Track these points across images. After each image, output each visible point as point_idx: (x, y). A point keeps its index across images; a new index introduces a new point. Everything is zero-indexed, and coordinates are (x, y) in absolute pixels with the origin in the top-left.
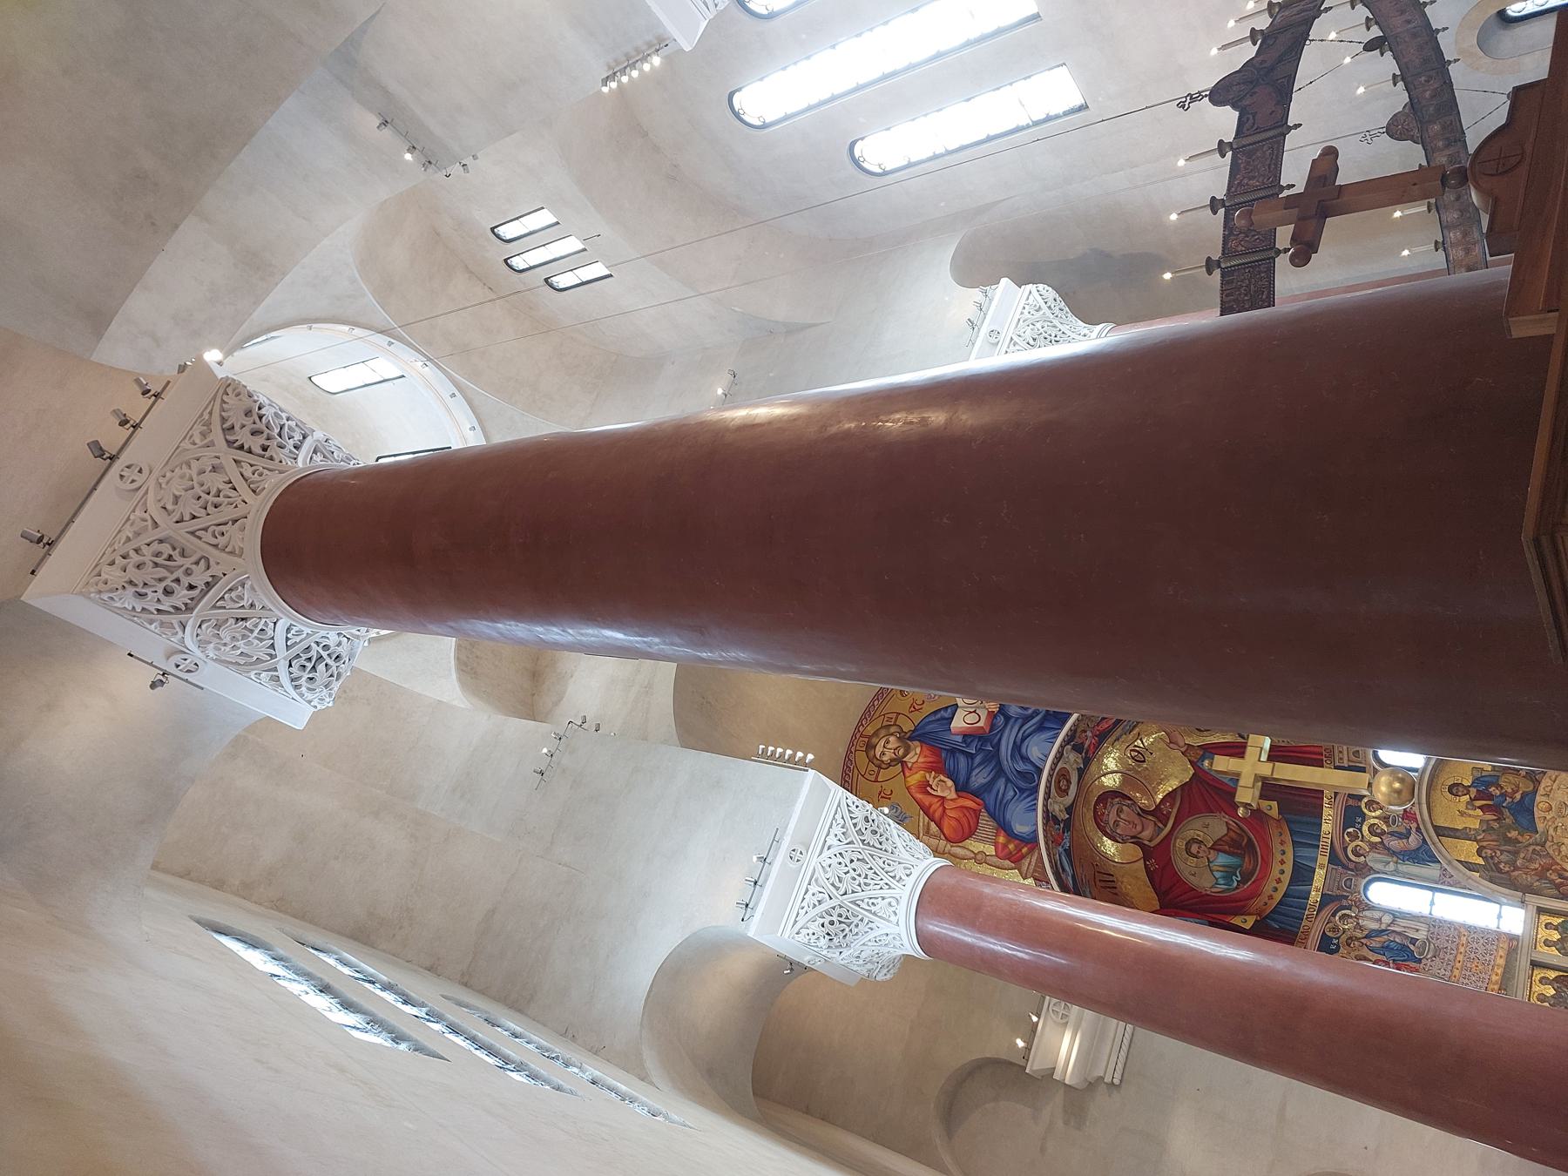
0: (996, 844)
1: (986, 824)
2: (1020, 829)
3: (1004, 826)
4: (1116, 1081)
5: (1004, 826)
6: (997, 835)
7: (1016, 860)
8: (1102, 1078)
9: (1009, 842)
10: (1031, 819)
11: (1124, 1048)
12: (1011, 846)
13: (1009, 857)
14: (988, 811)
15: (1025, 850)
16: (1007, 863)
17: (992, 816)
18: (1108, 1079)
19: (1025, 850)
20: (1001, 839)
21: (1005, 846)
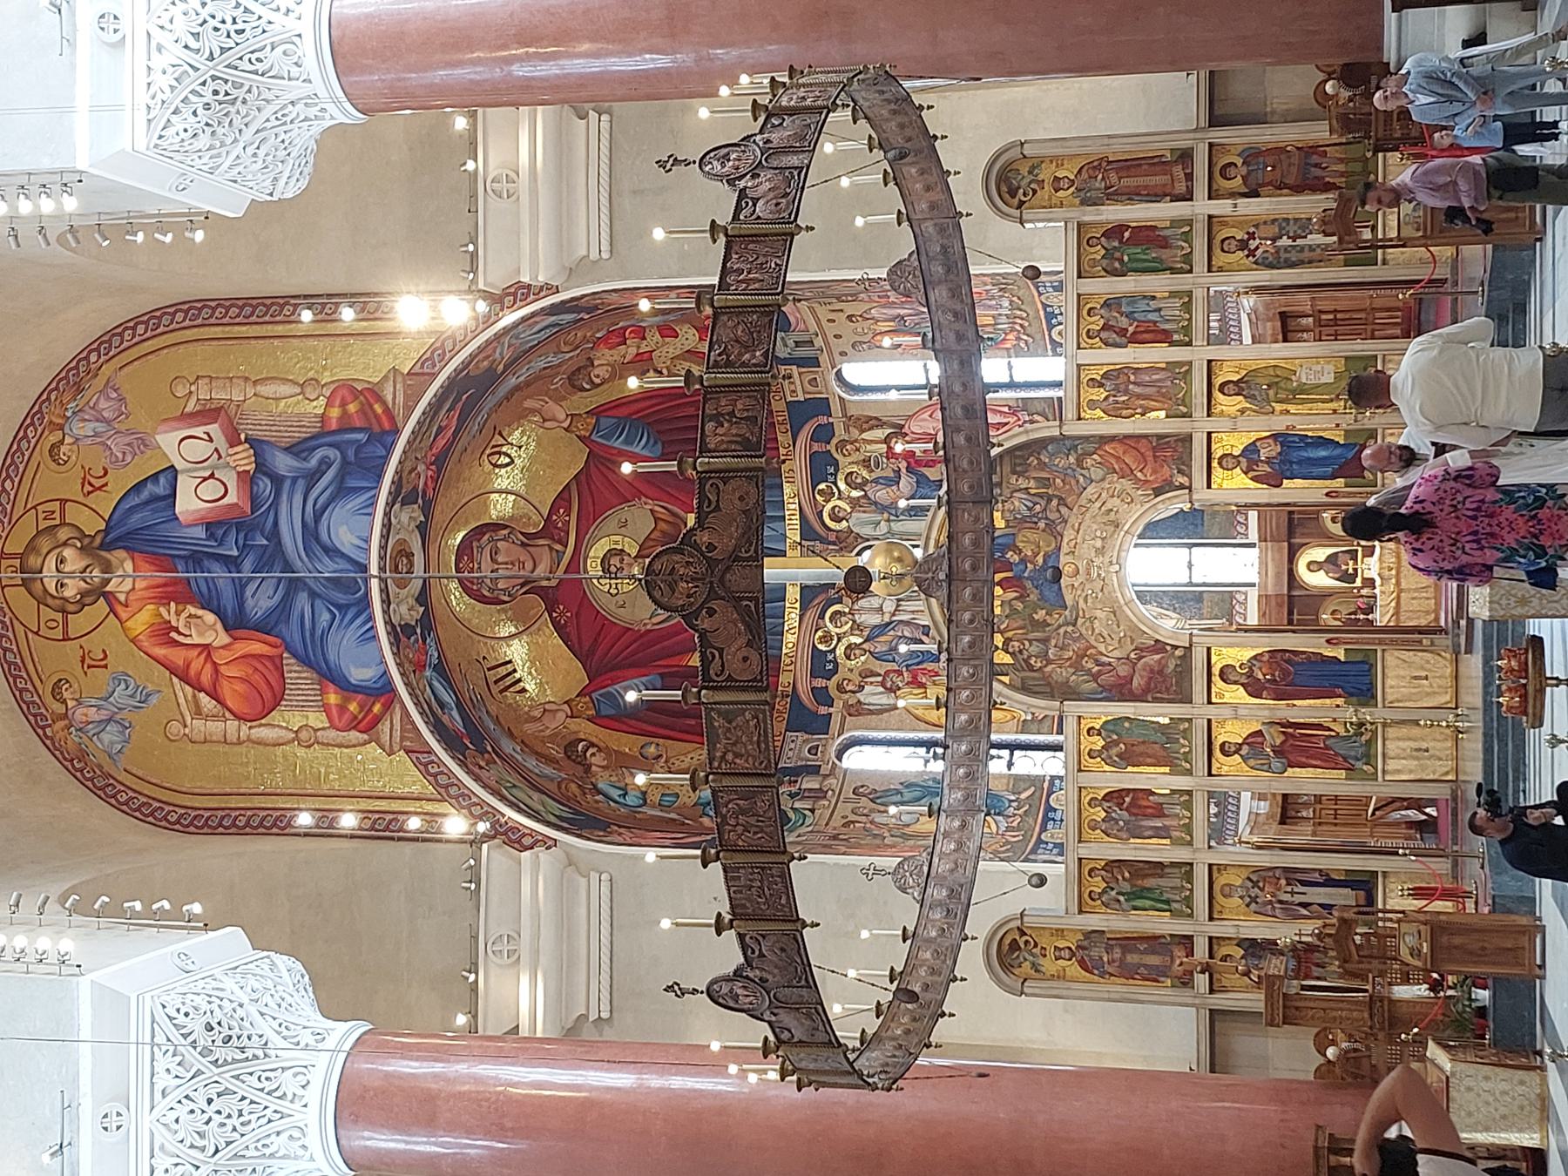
0: (326, 708)
1: (297, 676)
2: (360, 674)
3: (330, 676)
4: (605, 1015)
5: (330, 676)
6: (323, 692)
7: (368, 726)
8: (583, 1018)
9: (347, 700)
10: (372, 655)
11: (605, 967)
12: (353, 707)
13: (354, 724)
14: (294, 656)
15: (377, 708)
16: (354, 736)
17: (305, 661)
18: (593, 1016)
19: (377, 708)
20: (333, 699)
21: (342, 708)
